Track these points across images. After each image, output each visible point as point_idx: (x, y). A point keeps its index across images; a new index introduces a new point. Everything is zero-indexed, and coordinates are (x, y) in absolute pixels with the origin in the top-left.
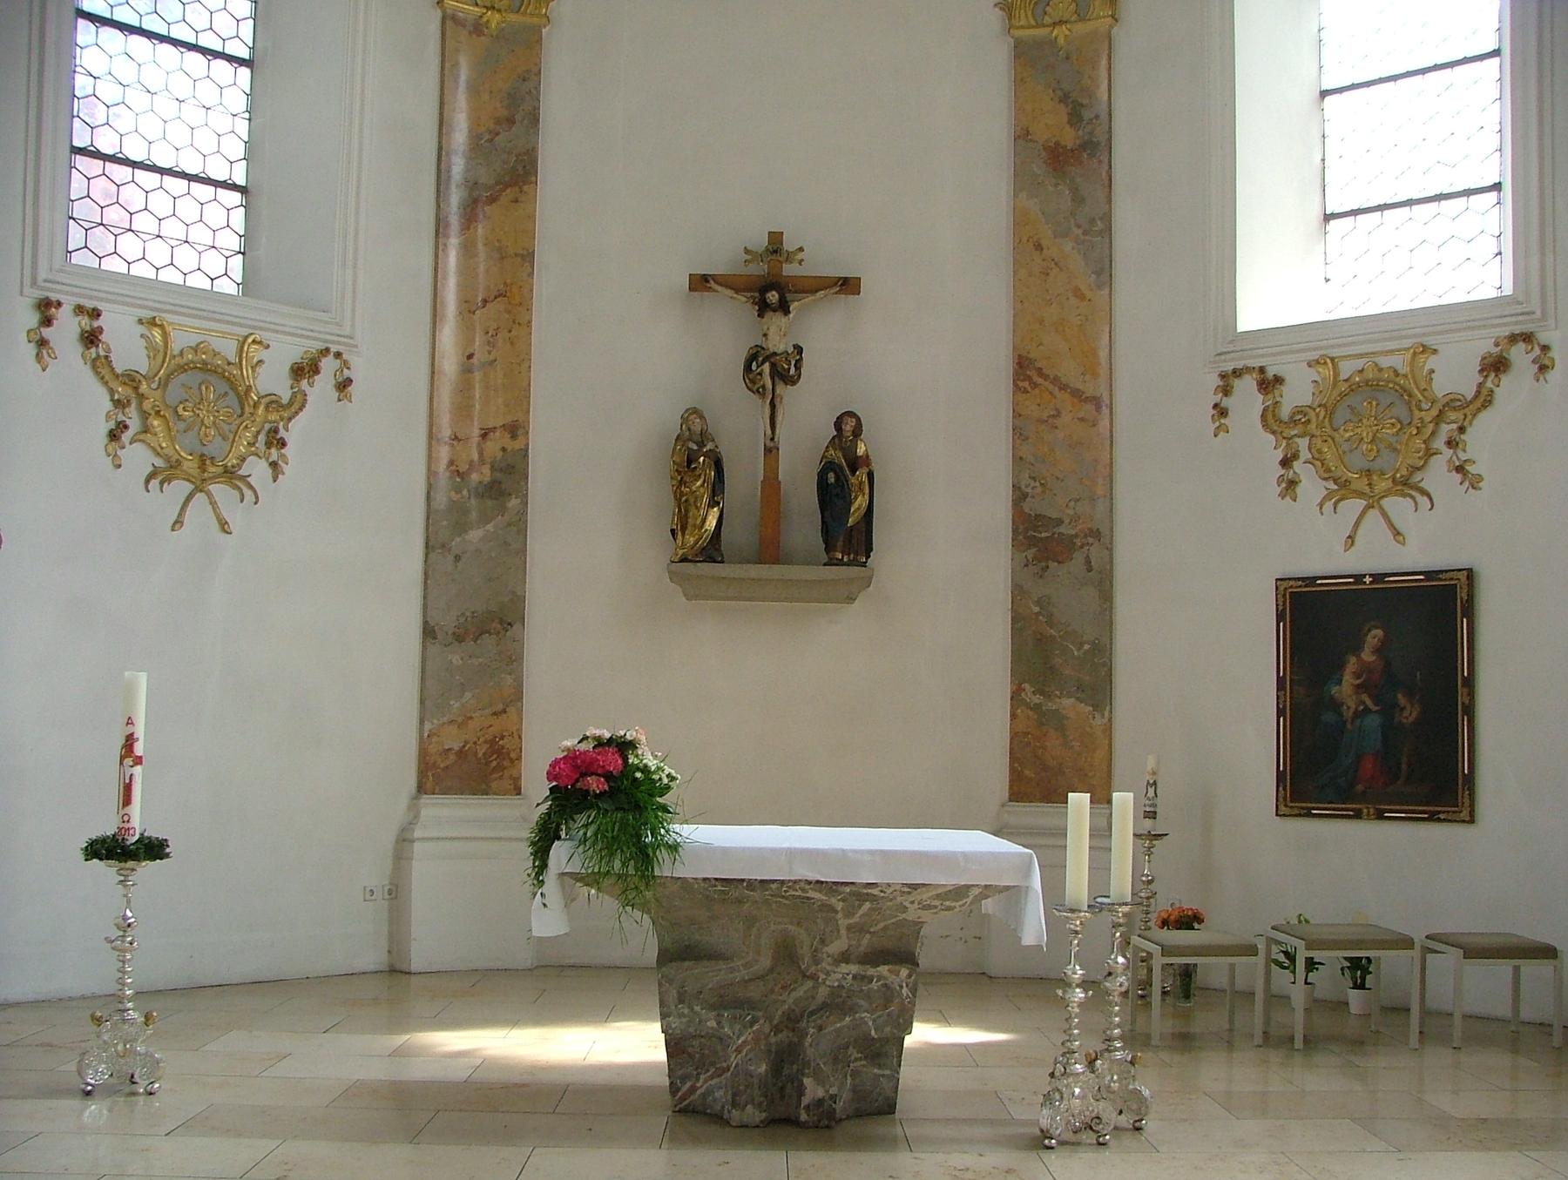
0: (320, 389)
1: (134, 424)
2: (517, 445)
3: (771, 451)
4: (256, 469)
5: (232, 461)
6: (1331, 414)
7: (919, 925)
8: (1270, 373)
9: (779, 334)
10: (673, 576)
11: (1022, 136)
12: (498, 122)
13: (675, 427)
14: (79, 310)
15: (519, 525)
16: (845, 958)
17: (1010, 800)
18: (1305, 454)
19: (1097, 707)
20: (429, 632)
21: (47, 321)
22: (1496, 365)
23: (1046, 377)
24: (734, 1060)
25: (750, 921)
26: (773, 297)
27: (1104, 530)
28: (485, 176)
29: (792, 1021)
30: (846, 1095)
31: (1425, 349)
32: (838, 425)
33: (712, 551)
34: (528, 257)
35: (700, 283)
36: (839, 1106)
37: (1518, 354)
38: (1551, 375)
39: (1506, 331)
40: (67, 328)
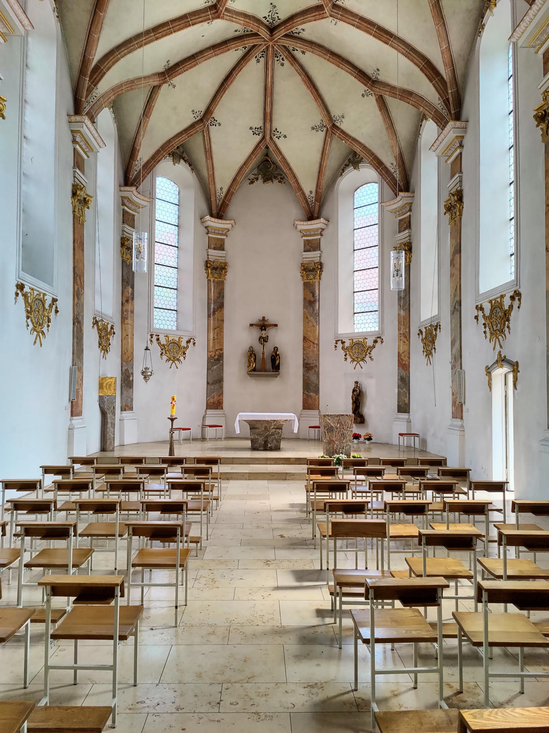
0: (191, 345)
1: (164, 352)
2: (222, 352)
3: (263, 353)
4: (182, 358)
5: (178, 357)
6: (352, 348)
7: (282, 425)
8: (343, 341)
10: (248, 374)
11: (305, 299)
12: (217, 297)
14: (156, 335)
15: (222, 365)
16: (273, 429)
17: (303, 409)
18: (348, 354)
19: (317, 394)
20: (208, 383)
21: (152, 337)
22: (376, 342)
23: (307, 339)
24: (260, 441)
25: (261, 424)
26: (263, 328)
27: (318, 365)
28: (216, 308)
29: (267, 437)
31: (366, 338)
32: (274, 349)
33: (254, 370)
34: (223, 320)
35: (251, 325)
36: (273, 448)
37: (379, 340)
40: (155, 337)
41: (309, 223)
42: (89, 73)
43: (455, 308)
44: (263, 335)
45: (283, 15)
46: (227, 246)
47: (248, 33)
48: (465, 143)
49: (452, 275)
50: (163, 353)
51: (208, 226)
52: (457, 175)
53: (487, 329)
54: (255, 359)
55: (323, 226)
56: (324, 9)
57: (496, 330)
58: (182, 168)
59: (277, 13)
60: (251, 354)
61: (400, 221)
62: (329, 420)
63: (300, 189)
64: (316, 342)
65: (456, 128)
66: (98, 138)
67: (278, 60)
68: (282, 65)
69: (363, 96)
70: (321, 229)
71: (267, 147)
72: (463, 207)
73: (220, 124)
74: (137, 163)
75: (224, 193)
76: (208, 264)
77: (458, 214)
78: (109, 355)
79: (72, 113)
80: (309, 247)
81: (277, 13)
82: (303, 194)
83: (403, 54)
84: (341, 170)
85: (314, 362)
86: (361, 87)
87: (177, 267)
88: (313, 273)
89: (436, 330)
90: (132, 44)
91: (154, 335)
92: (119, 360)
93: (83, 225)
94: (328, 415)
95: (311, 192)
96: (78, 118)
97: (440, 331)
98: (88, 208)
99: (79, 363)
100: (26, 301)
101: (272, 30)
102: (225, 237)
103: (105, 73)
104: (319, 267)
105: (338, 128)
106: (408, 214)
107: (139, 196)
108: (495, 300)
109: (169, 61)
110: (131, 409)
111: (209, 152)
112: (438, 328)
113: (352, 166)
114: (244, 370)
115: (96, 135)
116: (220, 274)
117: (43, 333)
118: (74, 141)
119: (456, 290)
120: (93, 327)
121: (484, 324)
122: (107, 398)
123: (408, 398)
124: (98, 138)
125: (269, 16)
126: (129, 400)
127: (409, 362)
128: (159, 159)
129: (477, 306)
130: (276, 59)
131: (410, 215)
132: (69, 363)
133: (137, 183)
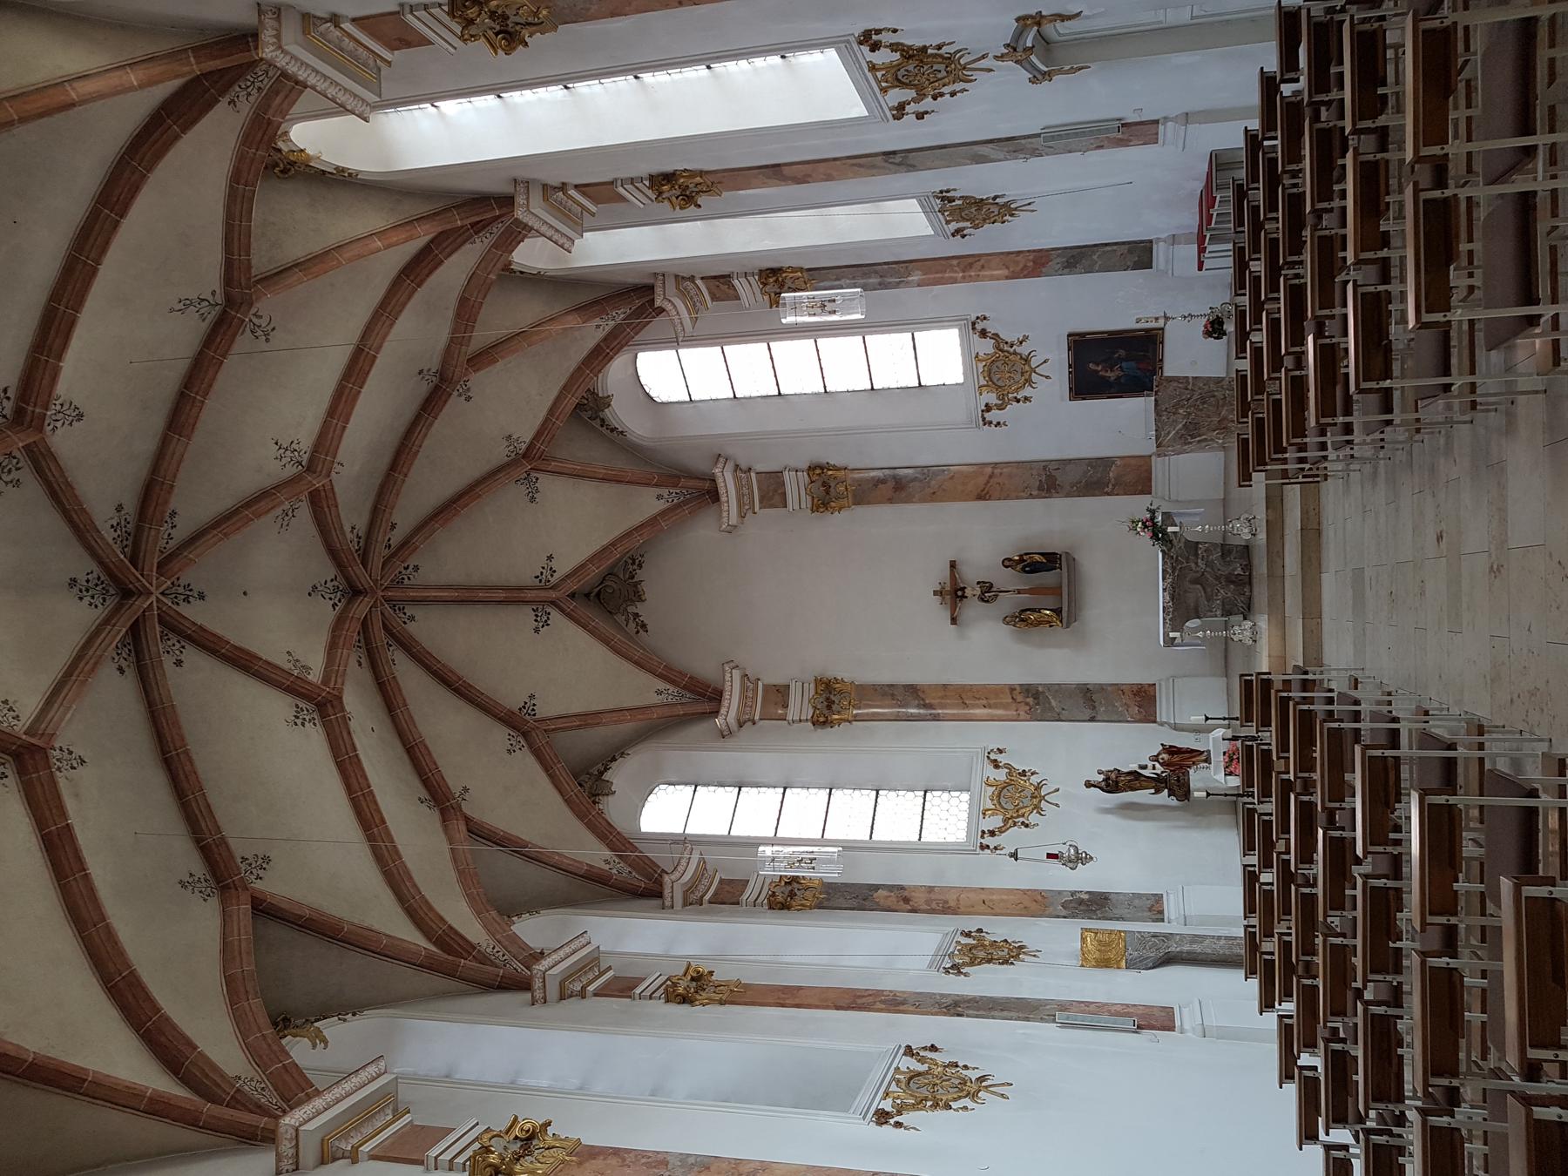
0: (1002, 759)
1: (1021, 819)
2: (1018, 688)
4: (1035, 780)
5: (1032, 788)
6: (1000, 387)
8: (983, 408)
9: (972, 591)
10: (1067, 627)
11: (891, 501)
13: (1007, 629)
14: (982, 837)
15: (1049, 687)
18: (1015, 395)
20: (1092, 720)
21: (988, 847)
22: (983, 333)
24: (1229, 594)
26: (960, 593)
29: (1217, 578)
30: (1241, 561)
31: (977, 357)
33: (1058, 611)
35: (954, 621)
37: (979, 327)
38: (987, 315)
39: (971, 331)
40: (988, 840)
41: (723, 499)
42: (450, 958)
43: (899, 164)
44: (975, 592)
45: (330, 571)
46: (779, 680)
47: (362, 640)
48: (555, 182)
49: (829, 178)
50: (1023, 823)
51: (739, 720)
52: (621, 190)
53: (946, 90)
54: (1033, 610)
55: (730, 466)
56: (317, 490)
57: (947, 72)
58: (620, 776)
59: (326, 583)
60: (1022, 619)
61: (714, 298)
62: (1169, 433)
63: (653, 522)
64: (989, 470)
65: (528, 202)
66: (573, 946)
67: (409, 578)
68: (416, 568)
69: (468, 399)
70: (735, 471)
71: (572, 596)
72: (685, 170)
73: (532, 697)
74: (614, 871)
75: (668, 687)
76: (822, 721)
77: (698, 179)
78: (1031, 947)
79: (528, 996)
80: (777, 498)
81: (326, 583)
82: (663, 513)
83: (391, 325)
84: (614, 436)
85: (1035, 472)
86: (454, 404)
87: (828, 790)
88: (832, 485)
89: (951, 200)
90: (395, 872)
91: (982, 841)
92: (1044, 922)
93: (747, 987)
94: (1157, 438)
95: (659, 497)
96: (537, 984)
97: (955, 190)
98: (711, 973)
99: (1048, 1007)
100: (914, 1107)
101: (354, 592)
102: (760, 683)
103: (450, 927)
104: (818, 472)
105: (531, 446)
106: (699, 282)
107: (680, 869)
108: (878, 82)
109: (420, 799)
110: (1158, 898)
111: (588, 719)
112: (948, 195)
113: (603, 411)
114: (1059, 632)
115: (567, 950)
116: (841, 692)
117: (982, 1079)
118: (582, 994)
119: (860, 166)
120: (966, 975)
121: (935, 98)
122: (1130, 951)
123: (1115, 247)
124: (573, 946)
125: (331, 599)
126: (1136, 902)
127: (1029, 251)
128: (604, 823)
129: (896, 118)
130: (406, 581)
131: (702, 278)
132: (1049, 1029)
133: (656, 872)
